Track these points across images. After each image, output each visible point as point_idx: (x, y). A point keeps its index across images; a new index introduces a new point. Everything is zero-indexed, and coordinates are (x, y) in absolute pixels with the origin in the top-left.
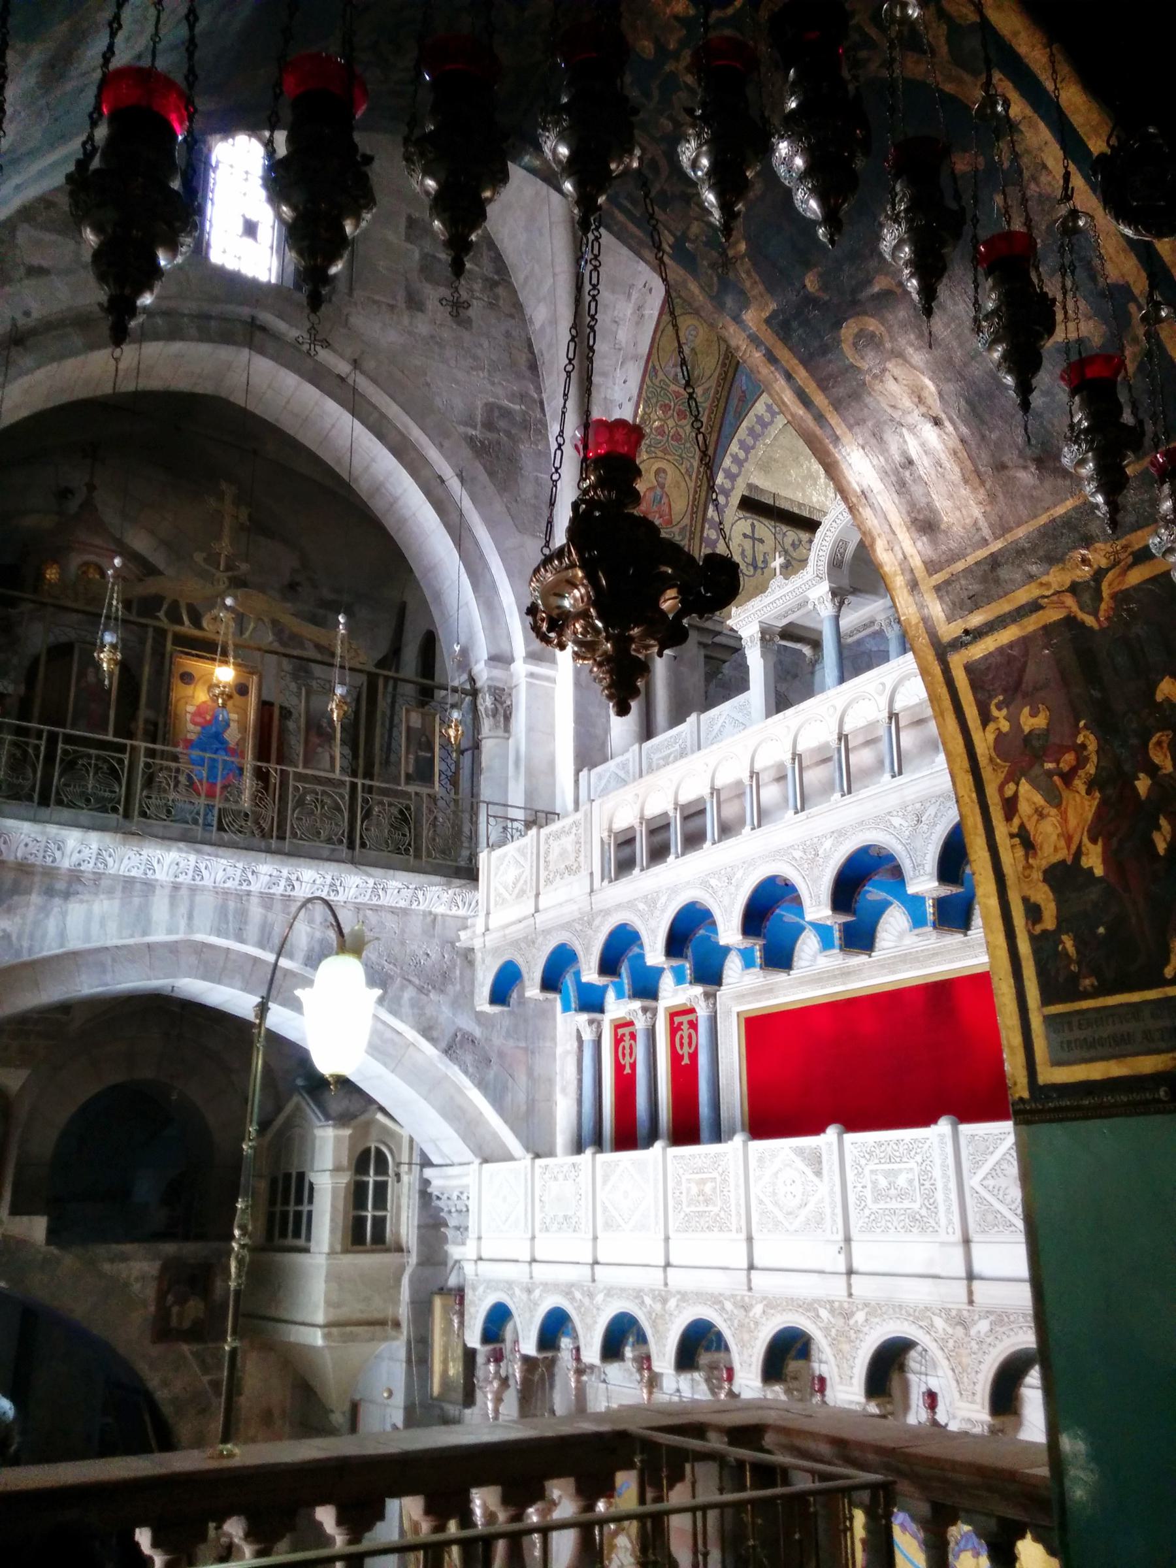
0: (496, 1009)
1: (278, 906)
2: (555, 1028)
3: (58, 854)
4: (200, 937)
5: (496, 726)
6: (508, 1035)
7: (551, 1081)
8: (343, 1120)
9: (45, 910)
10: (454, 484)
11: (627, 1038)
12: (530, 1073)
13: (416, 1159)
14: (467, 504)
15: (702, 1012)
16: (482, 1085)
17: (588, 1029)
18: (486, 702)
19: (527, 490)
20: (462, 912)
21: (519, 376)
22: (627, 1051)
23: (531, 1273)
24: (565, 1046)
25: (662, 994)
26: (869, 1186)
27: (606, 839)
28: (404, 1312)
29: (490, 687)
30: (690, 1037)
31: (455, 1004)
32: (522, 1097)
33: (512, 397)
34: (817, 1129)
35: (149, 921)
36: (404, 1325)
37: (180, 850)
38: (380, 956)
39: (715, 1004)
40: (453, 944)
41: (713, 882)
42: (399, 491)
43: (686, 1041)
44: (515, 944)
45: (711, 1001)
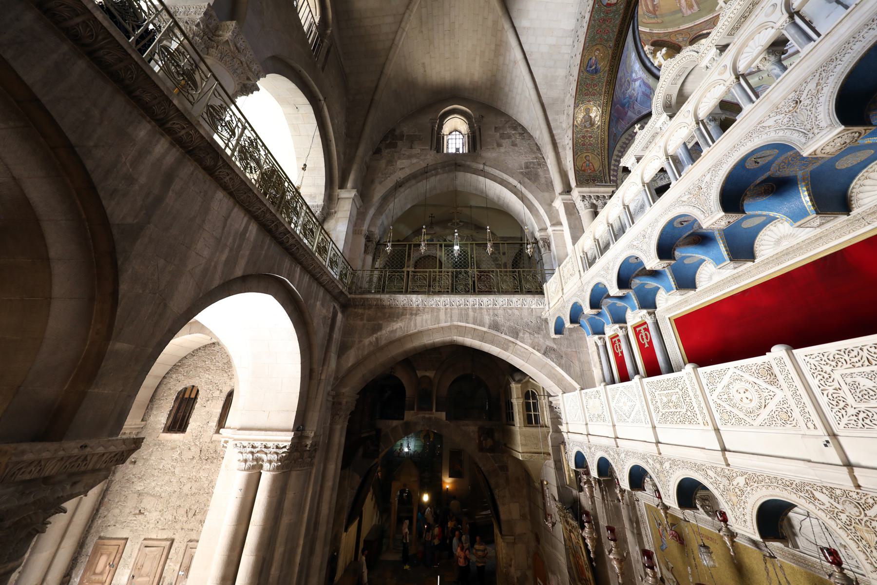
0: (558, 336)
1: (478, 311)
2: (587, 343)
3: (412, 303)
4: (455, 323)
5: (546, 250)
6: (567, 347)
7: (589, 363)
8: (519, 382)
9: (410, 319)
10: (519, 186)
11: (617, 342)
12: (579, 360)
13: (546, 394)
14: (524, 190)
15: (649, 321)
16: (560, 365)
17: (599, 341)
18: (541, 243)
19: (543, 180)
20: (542, 306)
21: (534, 153)
22: (618, 347)
23: (588, 440)
24: (592, 349)
25: (628, 321)
26: (845, 388)
27: (582, 256)
28: (551, 451)
29: (541, 239)
30: (646, 334)
31: (544, 337)
32: (578, 369)
33: (533, 158)
34: (762, 349)
35: (439, 320)
36: (552, 454)
37: (444, 297)
38: (514, 324)
39: (655, 316)
40: (540, 317)
41: (635, 243)
42: (504, 196)
43: (644, 337)
44: (559, 310)
45: (653, 315)
